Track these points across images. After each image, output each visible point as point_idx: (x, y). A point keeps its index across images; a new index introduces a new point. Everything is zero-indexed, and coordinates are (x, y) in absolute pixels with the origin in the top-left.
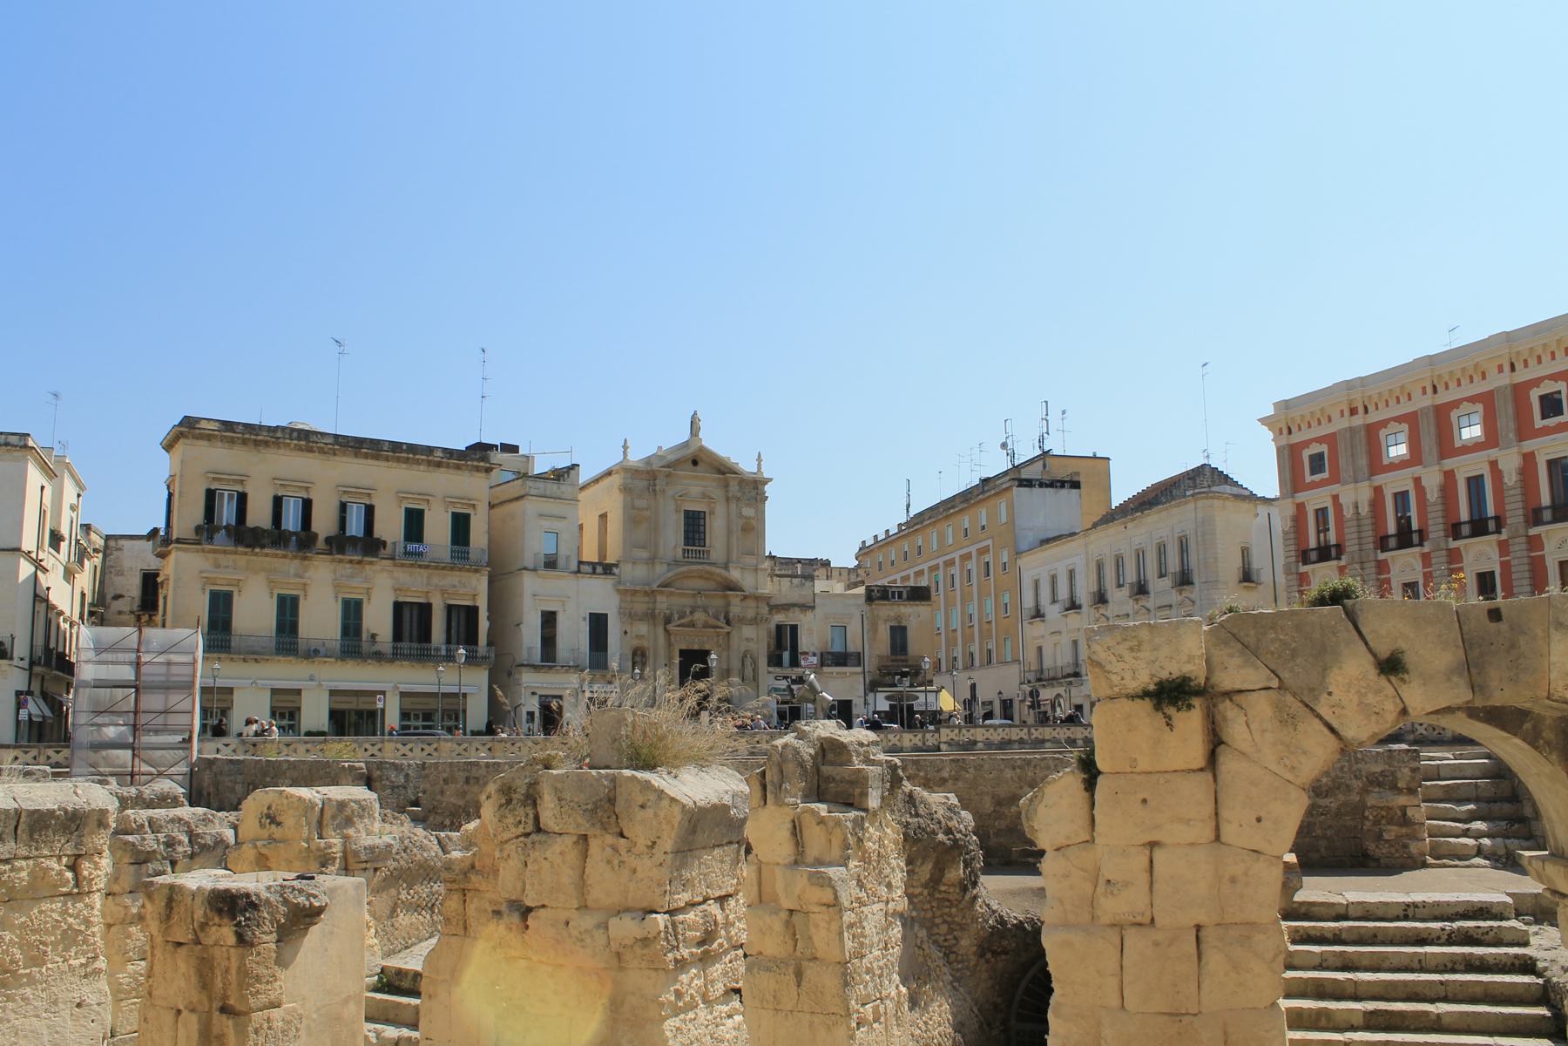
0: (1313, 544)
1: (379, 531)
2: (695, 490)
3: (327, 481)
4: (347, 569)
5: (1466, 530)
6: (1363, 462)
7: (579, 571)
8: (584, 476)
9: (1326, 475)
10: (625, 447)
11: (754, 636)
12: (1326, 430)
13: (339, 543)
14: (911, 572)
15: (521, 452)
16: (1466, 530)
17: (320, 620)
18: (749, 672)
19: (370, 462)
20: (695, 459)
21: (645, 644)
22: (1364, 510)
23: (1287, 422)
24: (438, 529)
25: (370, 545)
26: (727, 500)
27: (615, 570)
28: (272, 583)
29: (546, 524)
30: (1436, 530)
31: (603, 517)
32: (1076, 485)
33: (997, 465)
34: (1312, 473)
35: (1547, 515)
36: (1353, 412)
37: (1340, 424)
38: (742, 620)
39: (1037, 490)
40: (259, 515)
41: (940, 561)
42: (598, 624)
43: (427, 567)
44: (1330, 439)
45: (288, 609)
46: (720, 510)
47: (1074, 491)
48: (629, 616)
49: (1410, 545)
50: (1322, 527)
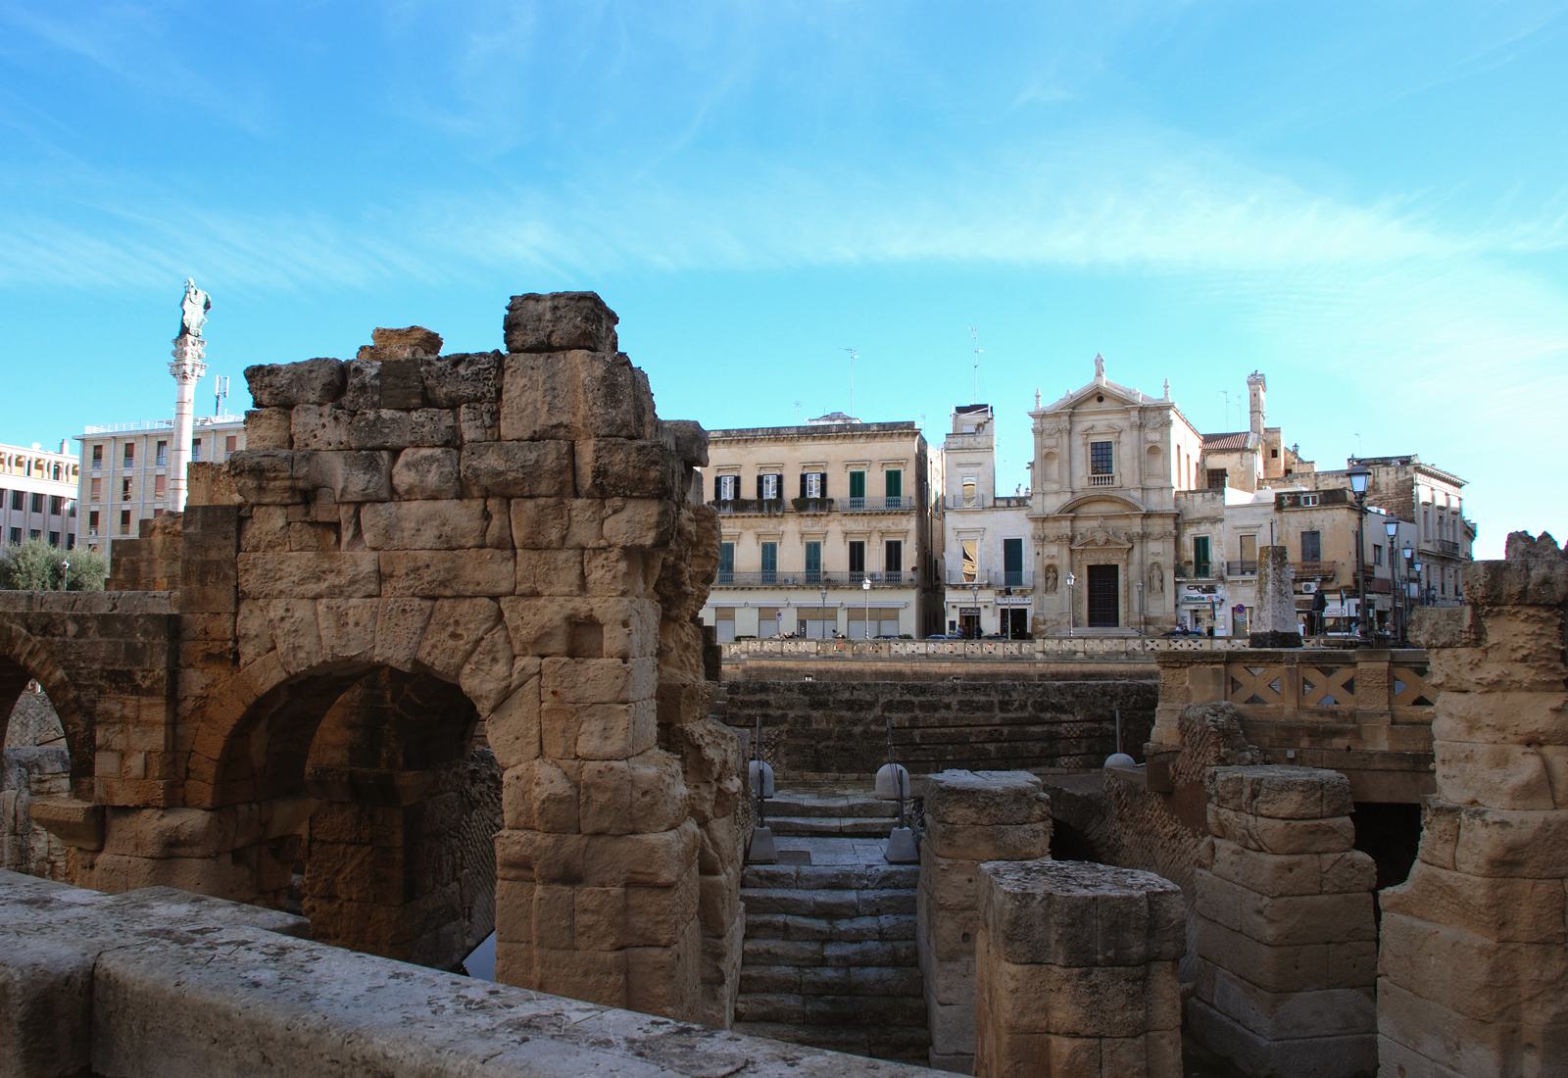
1: (831, 493)
2: (1099, 423)
3: (792, 459)
4: (809, 521)
7: (995, 506)
11: (1161, 550)
13: (802, 504)
17: (791, 560)
18: (1157, 584)
19: (823, 442)
21: (1056, 562)
24: (875, 487)
25: (824, 503)
27: (1029, 502)
40: (749, 492)
43: (864, 514)
46: (1124, 437)
48: (1042, 540)
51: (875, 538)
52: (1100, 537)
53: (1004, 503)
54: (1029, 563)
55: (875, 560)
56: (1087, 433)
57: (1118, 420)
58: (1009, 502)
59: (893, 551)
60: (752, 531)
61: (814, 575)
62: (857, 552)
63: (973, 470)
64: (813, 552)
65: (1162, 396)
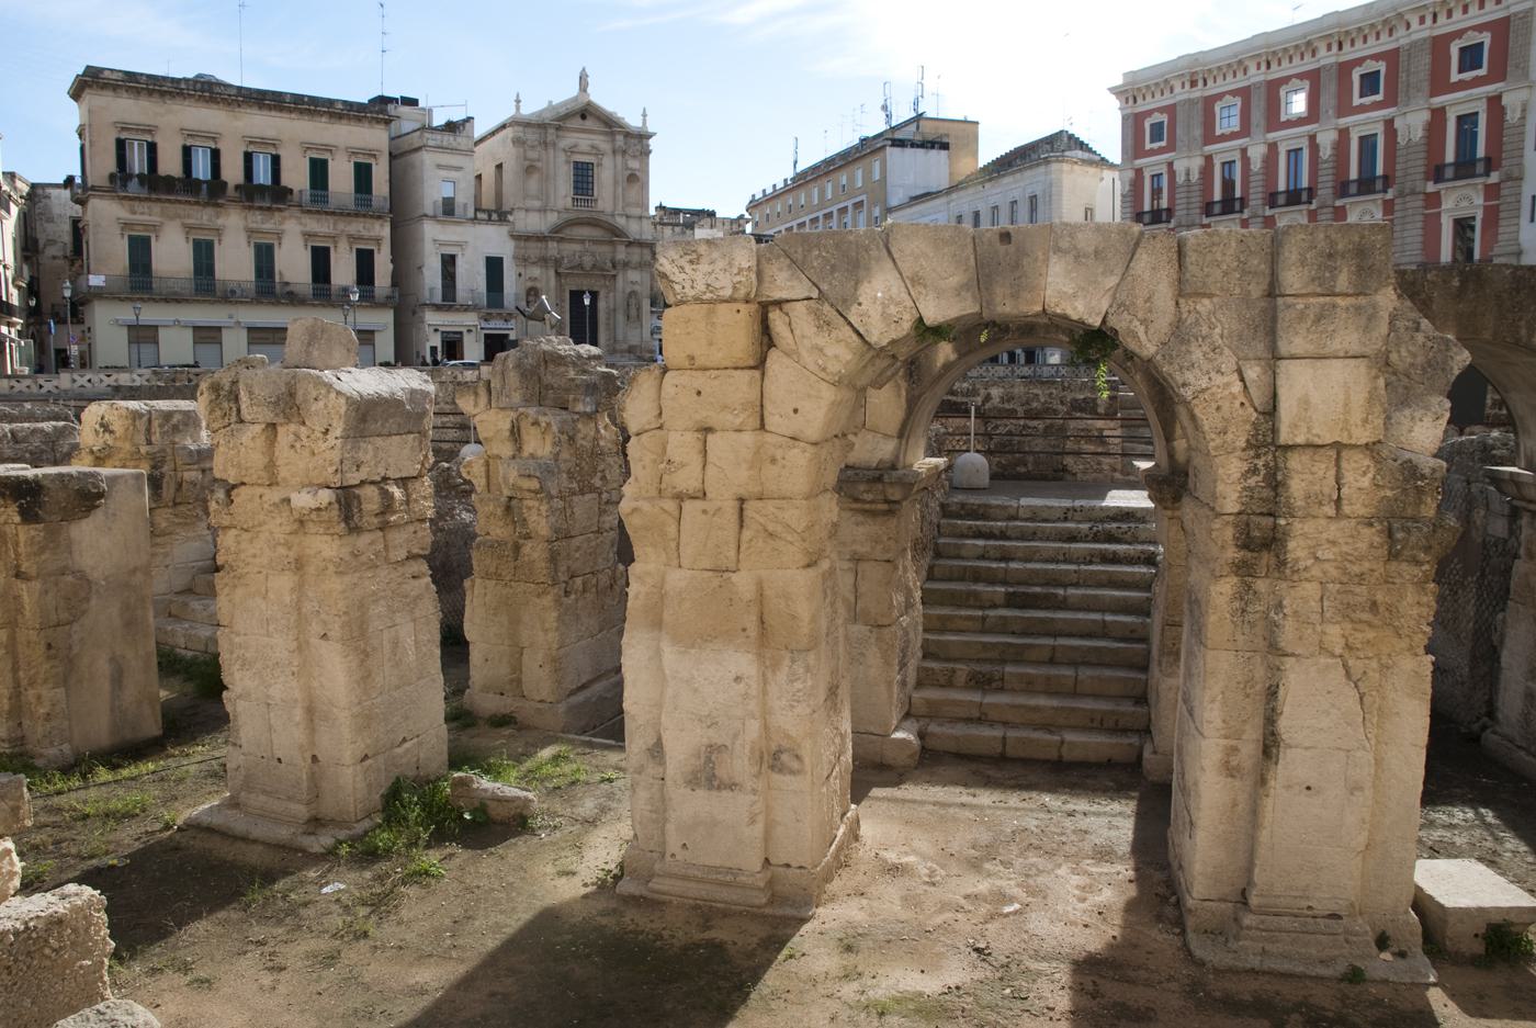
0: (1147, 208)
2: (584, 141)
5: (1281, 200)
6: (1198, 132)
8: (479, 130)
9: (1163, 144)
10: (518, 101)
12: (1167, 100)
13: (250, 193)
14: (794, 223)
15: (421, 104)
16: (1281, 200)
17: (235, 263)
18: (633, 312)
19: (273, 113)
20: (586, 112)
22: (1195, 177)
23: (1130, 92)
24: (341, 179)
25: (278, 194)
26: (614, 152)
27: (510, 218)
28: (188, 229)
29: (444, 173)
30: (1256, 199)
31: (499, 167)
32: (945, 146)
33: (875, 126)
34: (1152, 141)
35: (1353, 189)
36: (1193, 84)
37: (1182, 94)
38: (626, 265)
39: (909, 151)
40: (170, 165)
41: (820, 214)
42: (494, 266)
43: (333, 213)
44: (1170, 110)
45: (204, 254)
46: (607, 161)
47: (944, 153)
48: (522, 260)
49: (1232, 212)
50: (1156, 193)
51: (343, 245)
52: (588, 261)
53: (485, 216)
54: (511, 285)
55: (343, 271)
56: (571, 150)
57: (602, 142)
58: (490, 216)
59: (365, 261)
60: (177, 223)
61: (267, 287)
62: (321, 261)
63: (453, 175)
64: (264, 257)
65: (640, 125)
